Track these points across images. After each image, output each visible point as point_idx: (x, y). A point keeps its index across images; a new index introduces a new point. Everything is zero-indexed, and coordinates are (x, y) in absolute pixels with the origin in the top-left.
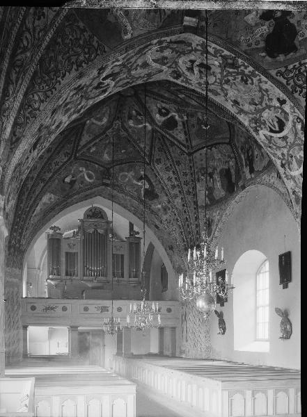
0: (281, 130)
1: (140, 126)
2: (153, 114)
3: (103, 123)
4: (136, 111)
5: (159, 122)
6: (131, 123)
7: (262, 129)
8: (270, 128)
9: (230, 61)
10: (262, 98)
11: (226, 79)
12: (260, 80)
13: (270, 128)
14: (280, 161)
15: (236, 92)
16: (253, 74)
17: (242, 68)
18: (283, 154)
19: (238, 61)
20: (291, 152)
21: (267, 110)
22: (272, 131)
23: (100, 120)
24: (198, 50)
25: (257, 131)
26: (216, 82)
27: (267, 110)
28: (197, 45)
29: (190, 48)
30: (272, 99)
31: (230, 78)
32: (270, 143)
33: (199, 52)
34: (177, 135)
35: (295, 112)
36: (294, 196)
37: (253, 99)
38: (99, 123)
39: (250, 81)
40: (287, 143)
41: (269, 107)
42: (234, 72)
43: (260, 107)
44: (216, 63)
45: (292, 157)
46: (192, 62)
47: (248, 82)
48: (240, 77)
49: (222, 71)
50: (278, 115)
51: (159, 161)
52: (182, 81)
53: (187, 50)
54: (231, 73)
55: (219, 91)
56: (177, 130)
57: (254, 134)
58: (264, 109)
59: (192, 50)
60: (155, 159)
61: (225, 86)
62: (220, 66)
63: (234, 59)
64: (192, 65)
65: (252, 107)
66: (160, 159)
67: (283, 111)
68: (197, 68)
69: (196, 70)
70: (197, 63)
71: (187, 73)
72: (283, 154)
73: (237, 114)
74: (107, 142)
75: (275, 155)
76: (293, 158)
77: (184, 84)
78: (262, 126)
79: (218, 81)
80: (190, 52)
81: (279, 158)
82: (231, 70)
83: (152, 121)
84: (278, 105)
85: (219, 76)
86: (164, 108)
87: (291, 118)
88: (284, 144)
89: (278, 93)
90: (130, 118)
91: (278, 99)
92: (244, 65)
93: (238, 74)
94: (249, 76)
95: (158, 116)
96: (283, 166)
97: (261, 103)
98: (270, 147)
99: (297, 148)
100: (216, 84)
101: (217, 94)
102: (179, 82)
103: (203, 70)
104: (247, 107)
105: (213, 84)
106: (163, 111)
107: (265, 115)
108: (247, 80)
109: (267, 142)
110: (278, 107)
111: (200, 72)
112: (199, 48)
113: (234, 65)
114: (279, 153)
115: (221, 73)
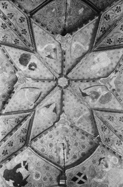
1: (46, 46)
2: (40, 62)
3: (75, 43)
4: (52, 58)
5: (33, 58)
6: (54, 46)
23: (78, 46)
34: (16, 53)
38: (78, 43)
51: (22, 20)
56: (18, 57)
60: (26, 20)
66: (22, 22)
74: (68, 17)
83: (40, 58)
86: (33, 70)
90: (55, 50)
95: (36, 62)
106: (33, 67)
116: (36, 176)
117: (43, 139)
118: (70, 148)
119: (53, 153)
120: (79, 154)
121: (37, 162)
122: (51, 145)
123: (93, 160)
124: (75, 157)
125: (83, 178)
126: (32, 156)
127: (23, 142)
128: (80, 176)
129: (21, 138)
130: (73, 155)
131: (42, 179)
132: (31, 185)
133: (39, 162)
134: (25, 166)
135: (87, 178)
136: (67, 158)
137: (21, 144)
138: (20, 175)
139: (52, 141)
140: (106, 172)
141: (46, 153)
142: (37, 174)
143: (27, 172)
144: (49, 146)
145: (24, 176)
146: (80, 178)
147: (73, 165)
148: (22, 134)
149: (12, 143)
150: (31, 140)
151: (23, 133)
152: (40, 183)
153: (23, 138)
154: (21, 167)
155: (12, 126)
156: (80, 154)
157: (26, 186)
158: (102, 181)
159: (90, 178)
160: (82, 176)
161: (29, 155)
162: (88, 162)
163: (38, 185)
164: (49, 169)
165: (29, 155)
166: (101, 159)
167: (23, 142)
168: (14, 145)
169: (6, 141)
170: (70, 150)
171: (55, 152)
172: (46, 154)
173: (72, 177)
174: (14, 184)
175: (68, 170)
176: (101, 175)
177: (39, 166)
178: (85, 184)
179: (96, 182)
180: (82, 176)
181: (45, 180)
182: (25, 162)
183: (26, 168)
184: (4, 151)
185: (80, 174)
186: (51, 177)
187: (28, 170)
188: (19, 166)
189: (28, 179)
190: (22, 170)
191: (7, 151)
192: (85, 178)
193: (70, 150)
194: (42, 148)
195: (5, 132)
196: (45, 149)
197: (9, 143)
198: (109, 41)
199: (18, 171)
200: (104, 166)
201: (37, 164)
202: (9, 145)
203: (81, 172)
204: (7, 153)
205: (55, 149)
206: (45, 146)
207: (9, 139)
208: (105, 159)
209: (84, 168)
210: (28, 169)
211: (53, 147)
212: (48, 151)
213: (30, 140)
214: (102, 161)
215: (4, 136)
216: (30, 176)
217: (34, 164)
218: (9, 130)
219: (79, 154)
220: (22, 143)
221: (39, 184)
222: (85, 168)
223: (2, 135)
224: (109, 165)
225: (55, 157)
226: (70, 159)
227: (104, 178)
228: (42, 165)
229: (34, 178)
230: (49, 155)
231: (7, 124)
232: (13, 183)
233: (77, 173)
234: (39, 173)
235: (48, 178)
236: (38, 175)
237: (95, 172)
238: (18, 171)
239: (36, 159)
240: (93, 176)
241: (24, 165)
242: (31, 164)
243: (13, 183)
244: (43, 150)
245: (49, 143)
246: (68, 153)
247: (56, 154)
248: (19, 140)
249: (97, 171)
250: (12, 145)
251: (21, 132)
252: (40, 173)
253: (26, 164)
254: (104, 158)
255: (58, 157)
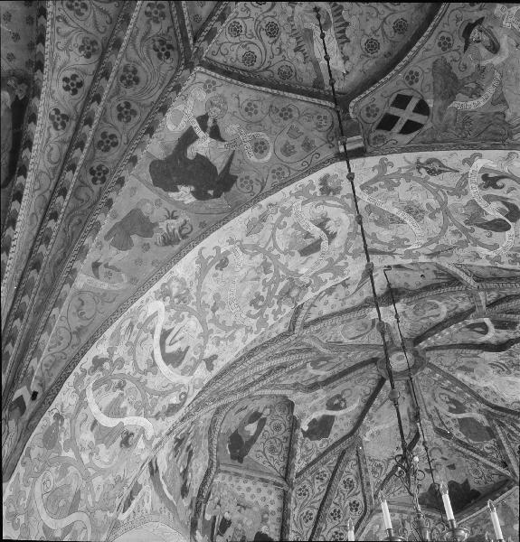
0: (171, 359)
7: (167, 309)
8: (171, 330)
9: (294, 293)
10: (223, 326)
11: (272, 268)
12: (251, 331)
13: (171, 330)
14: (106, 355)
15: (242, 273)
16: (263, 322)
17: (276, 307)
18: (121, 362)
19: (289, 304)
20: (129, 384)
21: (200, 330)
22: (165, 334)
24: (339, 260)
25: (164, 294)
26: (275, 246)
27: (200, 330)
28: (347, 264)
29: (350, 251)
30: (218, 344)
31: (269, 276)
32: (141, 327)
33: (336, 258)
35: (194, 387)
36: (52, 421)
37: (223, 305)
39: (254, 311)
40: (145, 373)
41: (205, 335)
42: (275, 289)
43: (210, 316)
44: (303, 270)
45: (120, 386)
46: (332, 237)
47: (252, 308)
48: (264, 294)
49: (288, 272)
50: (190, 354)
52: (312, 186)
53: (351, 244)
54: (276, 284)
55: (254, 238)
57: (157, 287)
58: (203, 323)
59: (346, 252)
61: (259, 259)
62: (296, 272)
63: (294, 300)
64: (327, 233)
65: (209, 299)
67: (197, 363)
68: (317, 236)
69: (317, 232)
70: (324, 244)
71: (320, 210)
72: (121, 362)
73: (200, 253)
75: (116, 337)
76: (119, 391)
77: (305, 181)
78: (173, 312)
79: (275, 252)
80: (347, 246)
81: (111, 351)
82: (281, 285)
84: (208, 354)
85: (283, 259)
87: (186, 380)
88: (143, 366)
89: (227, 356)
91: (215, 357)
92: (279, 312)
93: (270, 293)
94: (261, 314)
96: (98, 363)
97: (214, 320)
98: (131, 325)
99: (139, 398)
100: (271, 244)
101: (253, 228)
102: (315, 177)
103: (309, 242)
104: (211, 285)
105: (273, 235)
107: (192, 323)
108: (257, 307)
109: (141, 319)
110: (203, 353)
111: (308, 235)
112: (341, 263)
113: (286, 293)
114: (121, 351)
115: (284, 267)
116: (256, 151)
117: (237, 20)
118: (346, 18)
119: (291, 54)
120: (384, 33)
121: (245, 105)
122: (273, 31)
123: (443, 38)
124: (372, 46)
125: (414, 111)
126: (220, 91)
127: (168, 55)
128: (404, 108)
129: (157, 44)
130: (365, 40)
131: (279, 153)
132: (251, 182)
133: (249, 104)
134: (208, 129)
135: (431, 106)
136: (346, 59)
137: (167, 66)
138: (202, 162)
139: (271, 13)
140: (493, 67)
141: (263, 64)
142: (256, 144)
143: (222, 145)
144: (266, 39)
145: (219, 163)
146: (406, 115)
147: (370, 82)
148: (156, 29)
149: (135, 71)
150: (195, 40)
151: (157, 21)
152: (275, 167)
153: (162, 42)
154: (197, 138)
155: (105, 12)
156: (389, 29)
157: (234, 188)
158: (482, 104)
159: (440, 103)
160: (412, 105)
161: (208, 92)
162: (424, 56)
163: (271, 175)
164: (291, 116)
165: (208, 92)
166: (469, 28)
167: (168, 55)
168: (141, 75)
169: (112, 74)
170: (347, 24)
171: (295, 50)
172: (266, 69)
173: (377, 120)
174: (195, 194)
175: (357, 99)
176: (479, 86)
177: (254, 118)
178: (425, 128)
179: (464, 113)
180: (412, 105)
181: (288, 155)
182: (202, 120)
183: (215, 133)
184: (119, 108)
185: (401, 101)
186: (306, 138)
187: (224, 141)
188: (189, 137)
189: (232, 167)
190: (203, 146)
191: (128, 105)
192: (422, 108)
193: (347, 24)
194: (242, 51)
195: (94, 43)
196: (257, 53)
197: (123, 78)
198: (99, 174)
199: (191, 152)
200: (484, 51)
201: (246, 110)
202: (129, 84)
203: (408, 93)
204: (134, 113)
205: (293, 40)
206: (253, 40)
207: (117, 61)
208: (485, 25)
209: (412, 77)
210: (223, 135)
211: (284, 37)
212: (269, 53)
213: (191, 42)
214: (475, 34)
215: (94, 58)
216: (237, 156)
217: (238, 114)
218: (102, 29)
219: (384, 33)
220: (168, 61)
221: (273, 171)
222: (417, 74)
223: (88, 56)
224: (504, 42)
225: (301, 67)
226: (354, 59)
227: (490, 91)
228: (262, 108)
229: (253, 159)
230: (275, 69)
231: (83, 11)
232: (192, 192)
233: (392, 100)
234: (264, 136)
235: (297, 144)
236: (263, 143)
237: (455, 78)
238: (191, 152)
239: (238, 98)
240: (451, 96)
241: (204, 128)
242: (227, 116)
243: (192, 192)
244: (250, 58)
245: (264, 25)
246: (343, 39)
247: (300, 56)
248: (154, 54)
249: (460, 76)
250: (137, 80)
251: (148, 22)
252: (267, 138)
253: (210, 123)
254: (480, 21)
255: (310, 66)
